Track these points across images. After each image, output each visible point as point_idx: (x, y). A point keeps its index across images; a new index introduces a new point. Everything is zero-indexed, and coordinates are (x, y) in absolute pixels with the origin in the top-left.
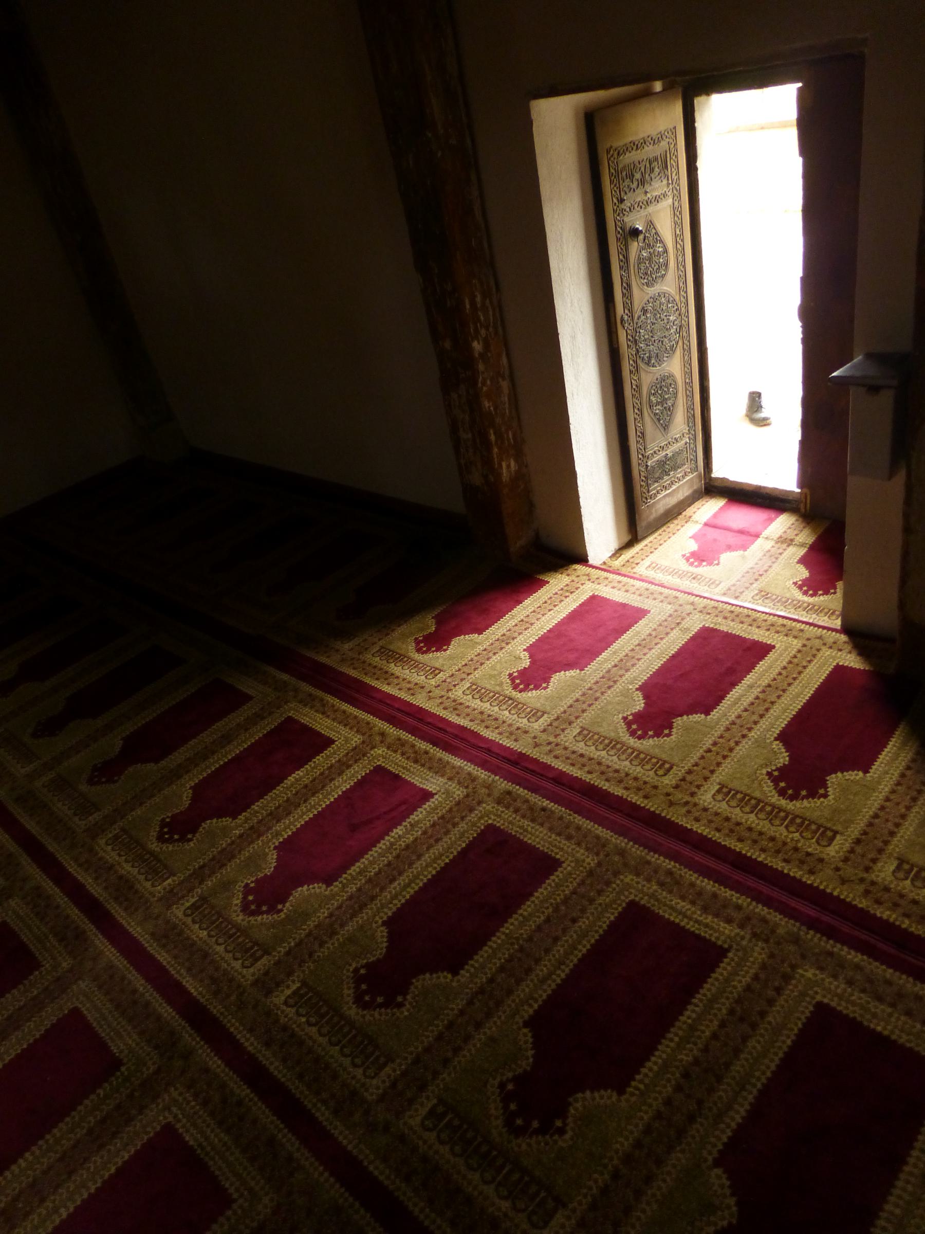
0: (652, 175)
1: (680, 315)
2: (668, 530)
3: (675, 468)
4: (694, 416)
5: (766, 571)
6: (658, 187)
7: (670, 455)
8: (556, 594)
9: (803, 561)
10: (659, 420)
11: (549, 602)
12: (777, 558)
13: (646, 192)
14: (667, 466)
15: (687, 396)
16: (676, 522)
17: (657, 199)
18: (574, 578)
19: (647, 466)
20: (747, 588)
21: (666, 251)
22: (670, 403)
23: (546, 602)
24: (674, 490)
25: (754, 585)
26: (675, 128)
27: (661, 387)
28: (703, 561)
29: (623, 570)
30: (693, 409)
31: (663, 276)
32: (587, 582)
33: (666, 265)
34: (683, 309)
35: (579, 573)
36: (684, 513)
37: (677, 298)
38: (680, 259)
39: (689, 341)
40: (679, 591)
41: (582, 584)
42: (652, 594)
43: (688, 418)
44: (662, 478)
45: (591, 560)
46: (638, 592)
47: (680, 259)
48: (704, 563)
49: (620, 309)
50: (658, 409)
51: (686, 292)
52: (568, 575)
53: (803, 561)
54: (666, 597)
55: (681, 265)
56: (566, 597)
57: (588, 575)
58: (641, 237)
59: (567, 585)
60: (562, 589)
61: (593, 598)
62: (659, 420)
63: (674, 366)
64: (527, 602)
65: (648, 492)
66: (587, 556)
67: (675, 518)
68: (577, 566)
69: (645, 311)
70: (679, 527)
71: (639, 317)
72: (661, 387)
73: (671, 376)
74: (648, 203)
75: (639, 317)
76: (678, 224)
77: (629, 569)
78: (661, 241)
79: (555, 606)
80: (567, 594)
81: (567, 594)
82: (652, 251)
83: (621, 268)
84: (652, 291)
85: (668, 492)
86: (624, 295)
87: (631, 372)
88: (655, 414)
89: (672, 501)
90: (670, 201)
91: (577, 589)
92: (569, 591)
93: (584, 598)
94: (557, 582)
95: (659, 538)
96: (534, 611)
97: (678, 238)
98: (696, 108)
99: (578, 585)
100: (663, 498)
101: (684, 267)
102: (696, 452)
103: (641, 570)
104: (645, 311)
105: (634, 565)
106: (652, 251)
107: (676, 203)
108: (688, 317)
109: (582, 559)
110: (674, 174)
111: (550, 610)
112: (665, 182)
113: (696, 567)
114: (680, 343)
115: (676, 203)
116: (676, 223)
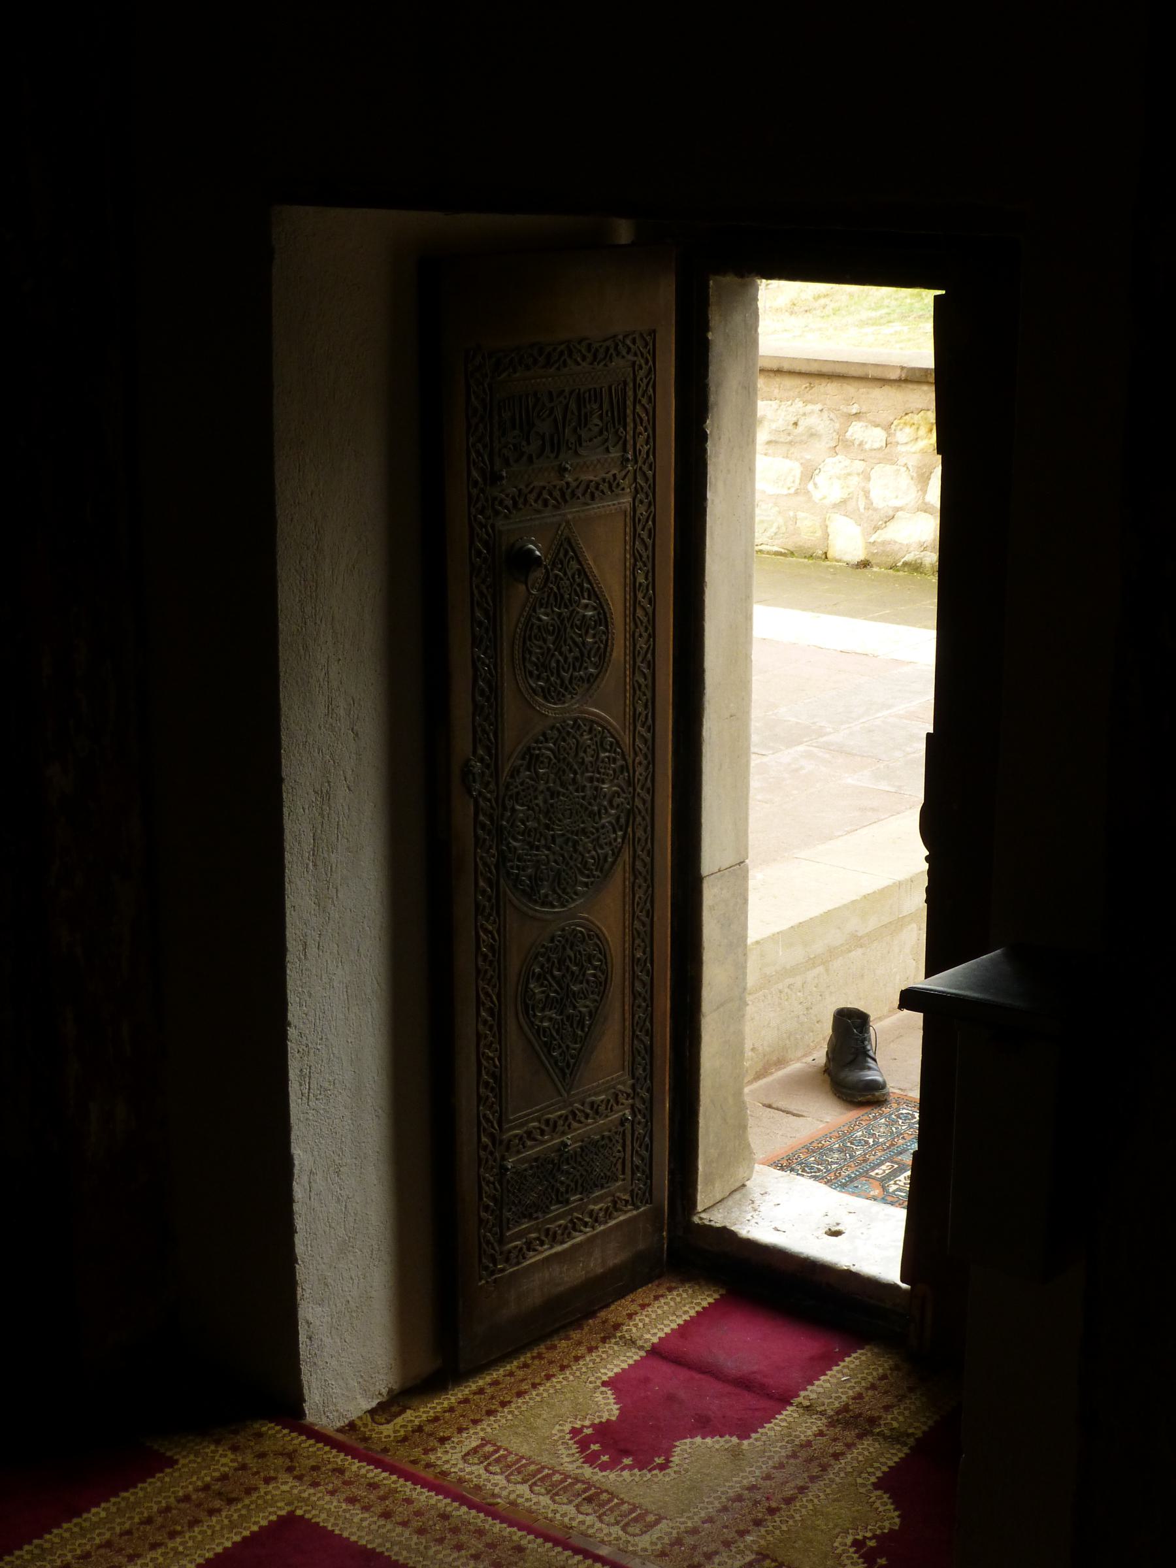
0: (584, 433)
1: (630, 782)
2: (548, 1355)
3: (585, 1186)
4: (650, 1050)
5: (789, 1501)
6: (597, 463)
7: (573, 1146)
8: (187, 1498)
9: (889, 1483)
10: (549, 1047)
11: (159, 1520)
12: (824, 1468)
13: (562, 470)
14: (564, 1178)
15: (635, 994)
16: (576, 1335)
17: (592, 492)
18: (249, 1459)
19: (504, 1169)
20: (727, 1544)
21: (603, 618)
22: (584, 1006)
23: (149, 1521)
24: (580, 1245)
25: (749, 1538)
26: (653, 333)
27: (561, 961)
28: (627, 1453)
29: (401, 1455)
30: (650, 1034)
31: (590, 680)
32: (283, 1476)
33: (603, 655)
34: (640, 770)
35: (267, 1445)
36: (602, 1314)
37: (627, 739)
38: (641, 643)
39: (651, 854)
40: (530, 1530)
41: (267, 1480)
42: (455, 1530)
43: (634, 1053)
44: (546, 1210)
45: (310, 1418)
46: (416, 1523)
47: (641, 643)
48: (627, 1461)
49: (462, 744)
50: (547, 1018)
51: (652, 729)
52: (235, 1449)
53: (889, 1483)
54: (492, 1546)
55: (642, 660)
56: (211, 1512)
57: (291, 1456)
58: (538, 574)
59: (224, 1477)
60: (206, 1488)
61: (289, 1522)
62: (549, 1047)
63: (606, 913)
64: (98, 1513)
65: (501, 1241)
66: (302, 1399)
67: (577, 1324)
68: (270, 1428)
69: (531, 758)
70: (582, 1350)
71: (515, 772)
72: (561, 961)
73: (593, 935)
74: (566, 496)
75: (515, 772)
76: (641, 557)
77: (417, 1452)
78: (594, 594)
79: (173, 1535)
80: (217, 1504)
81: (217, 1504)
82: (565, 612)
83: (476, 642)
84: (552, 710)
85: (559, 1248)
86: (477, 709)
87: (479, 909)
88: (539, 1031)
89: (572, 1275)
90: (626, 500)
91: (249, 1491)
92: (225, 1493)
93: (262, 1520)
94: (202, 1465)
95: (520, 1374)
96: (108, 1544)
97: (639, 594)
98: (712, 300)
99: (254, 1481)
100: (549, 1263)
101: (652, 665)
102: (649, 1148)
103: (452, 1459)
104: (531, 758)
105: (433, 1443)
106: (565, 612)
107: (642, 510)
108: (652, 791)
109: (286, 1405)
110: (641, 440)
111: (154, 1546)
112: (615, 454)
113: (603, 1467)
114: (626, 856)
115: (642, 510)
116: (636, 556)
